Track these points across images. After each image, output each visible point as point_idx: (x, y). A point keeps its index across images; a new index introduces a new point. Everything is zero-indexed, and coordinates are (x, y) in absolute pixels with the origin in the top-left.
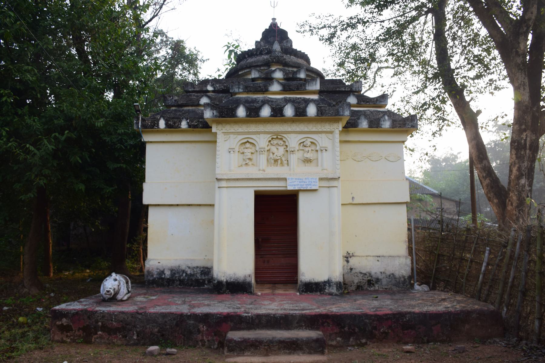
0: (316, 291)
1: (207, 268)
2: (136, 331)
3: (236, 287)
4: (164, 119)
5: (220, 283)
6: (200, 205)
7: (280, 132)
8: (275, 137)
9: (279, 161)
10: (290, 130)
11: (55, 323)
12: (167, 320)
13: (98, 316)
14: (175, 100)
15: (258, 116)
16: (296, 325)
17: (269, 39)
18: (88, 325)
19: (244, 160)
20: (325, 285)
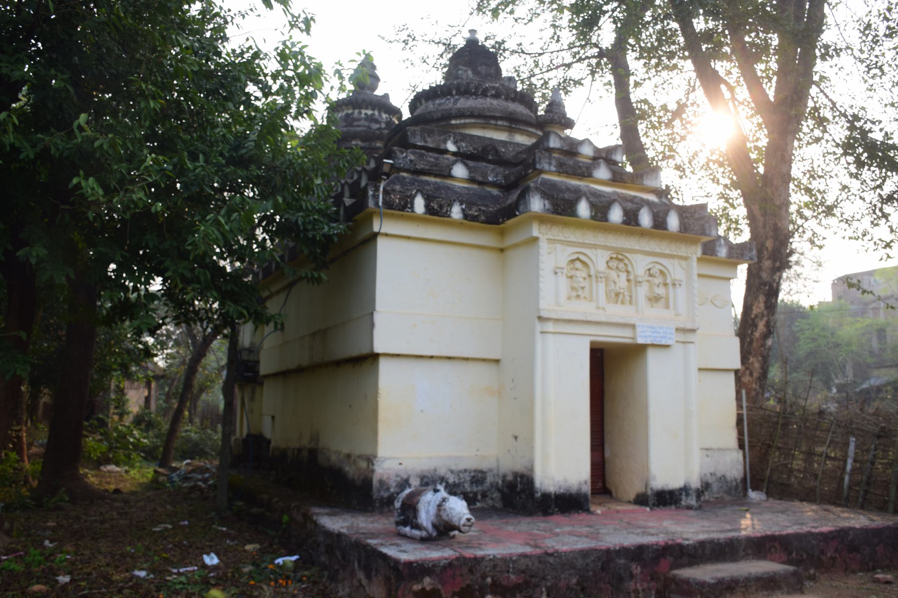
0: (670, 504)
1: (481, 472)
2: (546, 587)
3: (568, 503)
4: (423, 196)
5: (546, 496)
6: (467, 359)
7: (623, 248)
8: (614, 256)
9: (621, 297)
10: (637, 247)
11: (411, 588)
12: (588, 561)
13: (486, 567)
14: (411, 161)
15: (607, 220)
16: (742, 553)
17: (479, 68)
18: (468, 586)
19: (573, 288)
20: (681, 494)
